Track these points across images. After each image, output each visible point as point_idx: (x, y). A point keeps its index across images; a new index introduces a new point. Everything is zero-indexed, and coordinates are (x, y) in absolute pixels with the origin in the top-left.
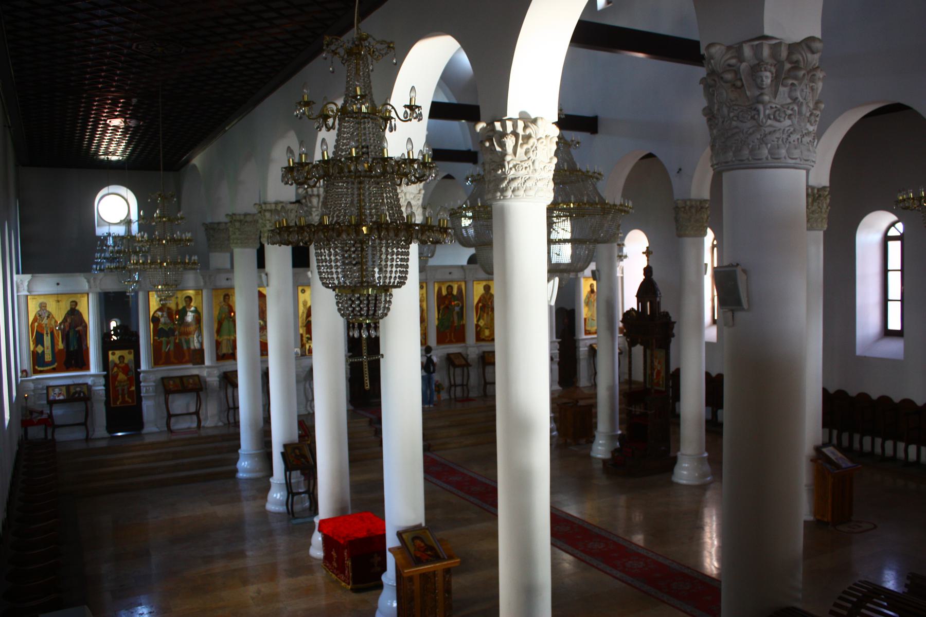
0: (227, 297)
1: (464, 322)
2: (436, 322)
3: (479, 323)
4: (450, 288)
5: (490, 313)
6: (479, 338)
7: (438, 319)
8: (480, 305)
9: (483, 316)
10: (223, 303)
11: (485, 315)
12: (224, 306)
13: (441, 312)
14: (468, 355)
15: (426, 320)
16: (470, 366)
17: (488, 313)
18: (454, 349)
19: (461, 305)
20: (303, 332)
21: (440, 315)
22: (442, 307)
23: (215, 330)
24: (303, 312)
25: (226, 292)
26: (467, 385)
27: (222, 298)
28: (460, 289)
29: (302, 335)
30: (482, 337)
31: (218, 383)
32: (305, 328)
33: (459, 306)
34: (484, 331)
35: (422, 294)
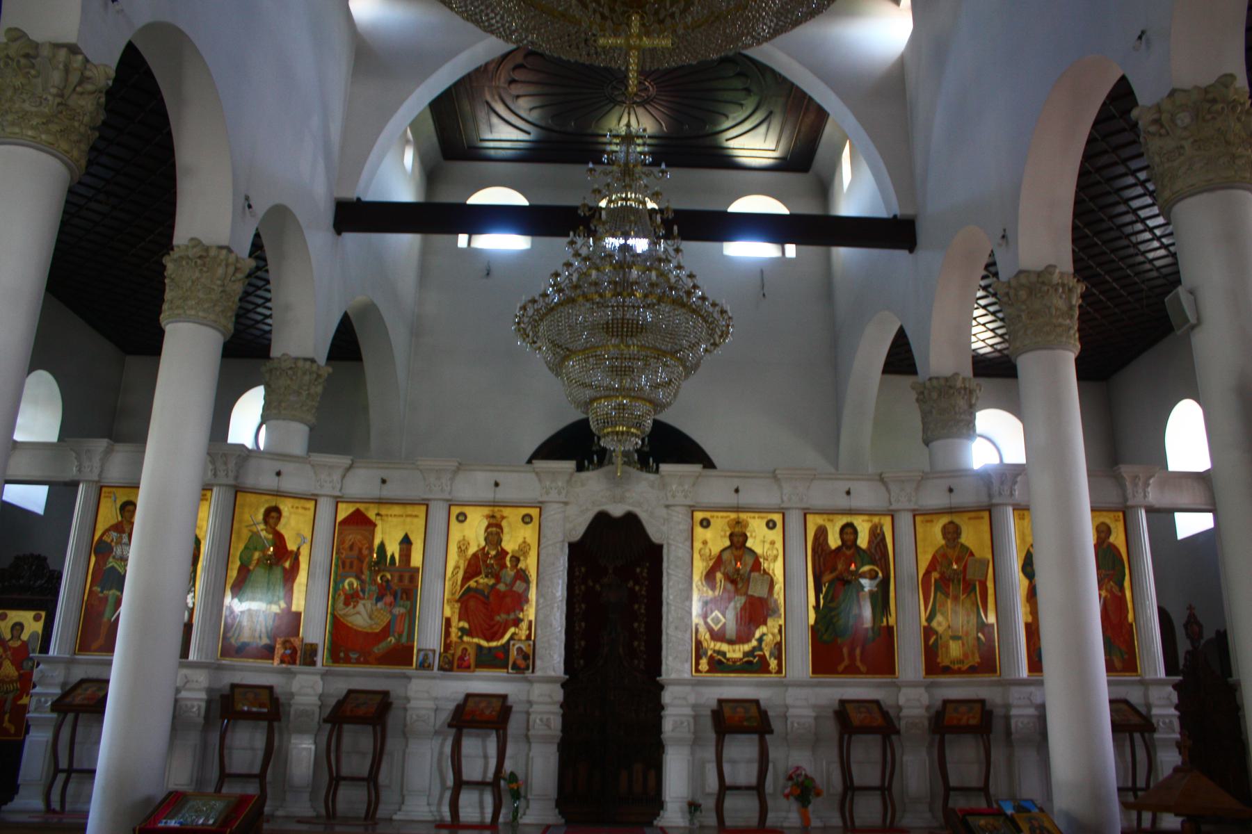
0: (274, 514)
1: (892, 621)
3: (934, 624)
4: (849, 531)
5: (962, 597)
6: (934, 664)
7: (817, 607)
8: (935, 575)
9: (943, 604)
10: (262, 526)
11: (949, 602)
12: (263, 534)
13: (824, 590)
14: (900, 708)
16: (898, 732)
17: (956, 599)
18: (859, 689)
19: (880, 575)
20: (453, 613)
21: (821, 596)
22: (827, 577)
23: (230, 581)
24: (457, 567)
25: (273, 504)
26: (890, 788)
27: (260, 517)
28: (877, 536)
29: (448, 622)
30: (943, 660)
31: (203, 705)
32: (457, 606)
33: (876, 576)
34: (947, 647)
35: (773, 543)
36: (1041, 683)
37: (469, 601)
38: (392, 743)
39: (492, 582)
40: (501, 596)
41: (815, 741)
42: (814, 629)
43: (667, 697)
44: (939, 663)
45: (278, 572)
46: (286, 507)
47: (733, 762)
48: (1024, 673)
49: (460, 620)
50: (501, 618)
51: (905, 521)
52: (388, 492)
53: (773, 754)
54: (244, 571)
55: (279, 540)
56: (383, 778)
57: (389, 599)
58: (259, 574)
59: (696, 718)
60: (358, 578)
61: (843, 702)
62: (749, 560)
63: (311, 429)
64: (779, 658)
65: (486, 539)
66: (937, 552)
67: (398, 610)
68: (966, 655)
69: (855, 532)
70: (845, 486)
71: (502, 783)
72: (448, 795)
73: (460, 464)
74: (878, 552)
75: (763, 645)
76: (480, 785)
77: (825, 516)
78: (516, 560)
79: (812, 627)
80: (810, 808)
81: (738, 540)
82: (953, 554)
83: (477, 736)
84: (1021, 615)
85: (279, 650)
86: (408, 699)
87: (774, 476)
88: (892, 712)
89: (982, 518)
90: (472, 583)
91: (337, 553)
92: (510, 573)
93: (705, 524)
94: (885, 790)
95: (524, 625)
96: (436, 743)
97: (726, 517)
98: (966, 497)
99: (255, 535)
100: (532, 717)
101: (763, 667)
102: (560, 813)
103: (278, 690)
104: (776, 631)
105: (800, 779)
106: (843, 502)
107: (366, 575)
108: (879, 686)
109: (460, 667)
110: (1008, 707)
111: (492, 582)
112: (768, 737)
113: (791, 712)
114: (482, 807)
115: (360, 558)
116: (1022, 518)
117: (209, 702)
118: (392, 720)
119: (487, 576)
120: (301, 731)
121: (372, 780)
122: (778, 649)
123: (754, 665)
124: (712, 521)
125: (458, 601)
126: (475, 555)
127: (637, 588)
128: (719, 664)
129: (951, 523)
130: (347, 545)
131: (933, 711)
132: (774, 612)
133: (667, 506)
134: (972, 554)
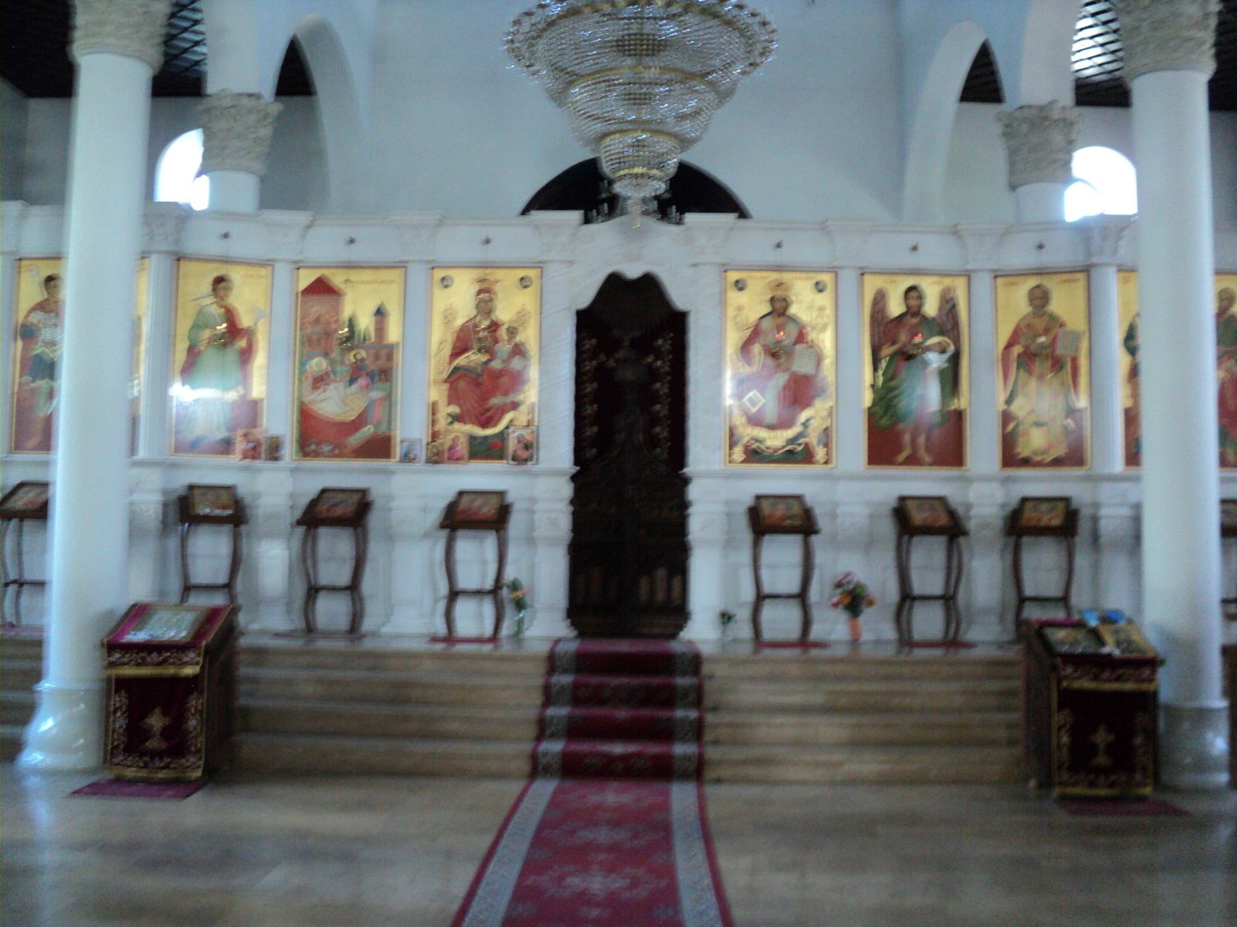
0: (222, 285)
2: (867, 399)
6: (1011, 458)
7: (873, 386)
8: (1017, 350)
10: (211, 300)
13: (883, 364)
15: (832, 390)
16: (965, 533)
19: (952, 348)
22: (887, 351)
28: (949, 305)
29: (434, 409)
30: (1023, 450)
32: (446, 387)
36: (1137, 479)
37: (458, 381)
38: (375, 548)
39: (484, 358)
40: (496, 376)
41: (868, 544)
42: (871, 414)
43: (694, 492)
44: (1018, 454)
45: (231, 354)
46: (236, 275)
47: (773, 567)
48: (1117, 464)
49: (449, 404)
50: (496, 401)
51: (983, 283)
52: (355, 254)
53: (820, 558)
54: (193, 353)
55: (230, 317)
56: (367, 585)
57: (362, 381)
58: (210, 357)
59: (729, 515)
60: (326, 355)
61: (903, 499)
62: (793, 331)
63: (263, 180)
64: (826, 445)
65: (477, 307)
66: (1020, 321)
67: (375, 394)
68: (1050, 446)
69: (920, 297)
70: (911, 240)
71: (505, 592)
72: (442, 605)
73: (443, 217)
74: (948, 323)
75: (810, 429)
76: (478, 593)
77: (886, 277)
78: (512, 332)
79: (869, 409)
80: (862, 619)
81: (779, 308)
82: (1040, 324)
83: (475, 538)
84: (1119, 398)
85: (240, 446)
86: (390, 498)
87: (823, 227)
88: (960, 511)
89: (1075, 281)
90: (461, 361)
91: (301, 329)
92: (504, 348)
93: (740, 286)
94: (948, 599)
95: (523, 409)
96: (425, 546)
97: (766, 278)
98: (1058, 255)
99: (201, 312)
100: (536, 516)
101: (806, 456)
102: (573, 624)
103: (242, 491)
104: (824, 413)
105: (851, 587)
106: (910, 261)
107: (335, 355)
108: (948, 479)
109: (449, 459)
110: (1096, 505)
111: (484, 358)
112: (814, 539)
113: (840, 510)
114: (480, 616)
115: (328, 334)
116: (1126, 281)
117: (165, 505)
118: (374, 520)
119: (479, 351)
120: (270, 535)
121: (353, 588)
122: (826, 437)
123: (797, 455)
124: (749, 282)
125: (446, 381)
126: (463, 328)
127: (659, 363)
128: (755, 455)
129: (1038, 287)
130: (312, 318)
131: (1009, 510)
132: (822, 392)
133: (695, 265)
134: (1062, 325)
